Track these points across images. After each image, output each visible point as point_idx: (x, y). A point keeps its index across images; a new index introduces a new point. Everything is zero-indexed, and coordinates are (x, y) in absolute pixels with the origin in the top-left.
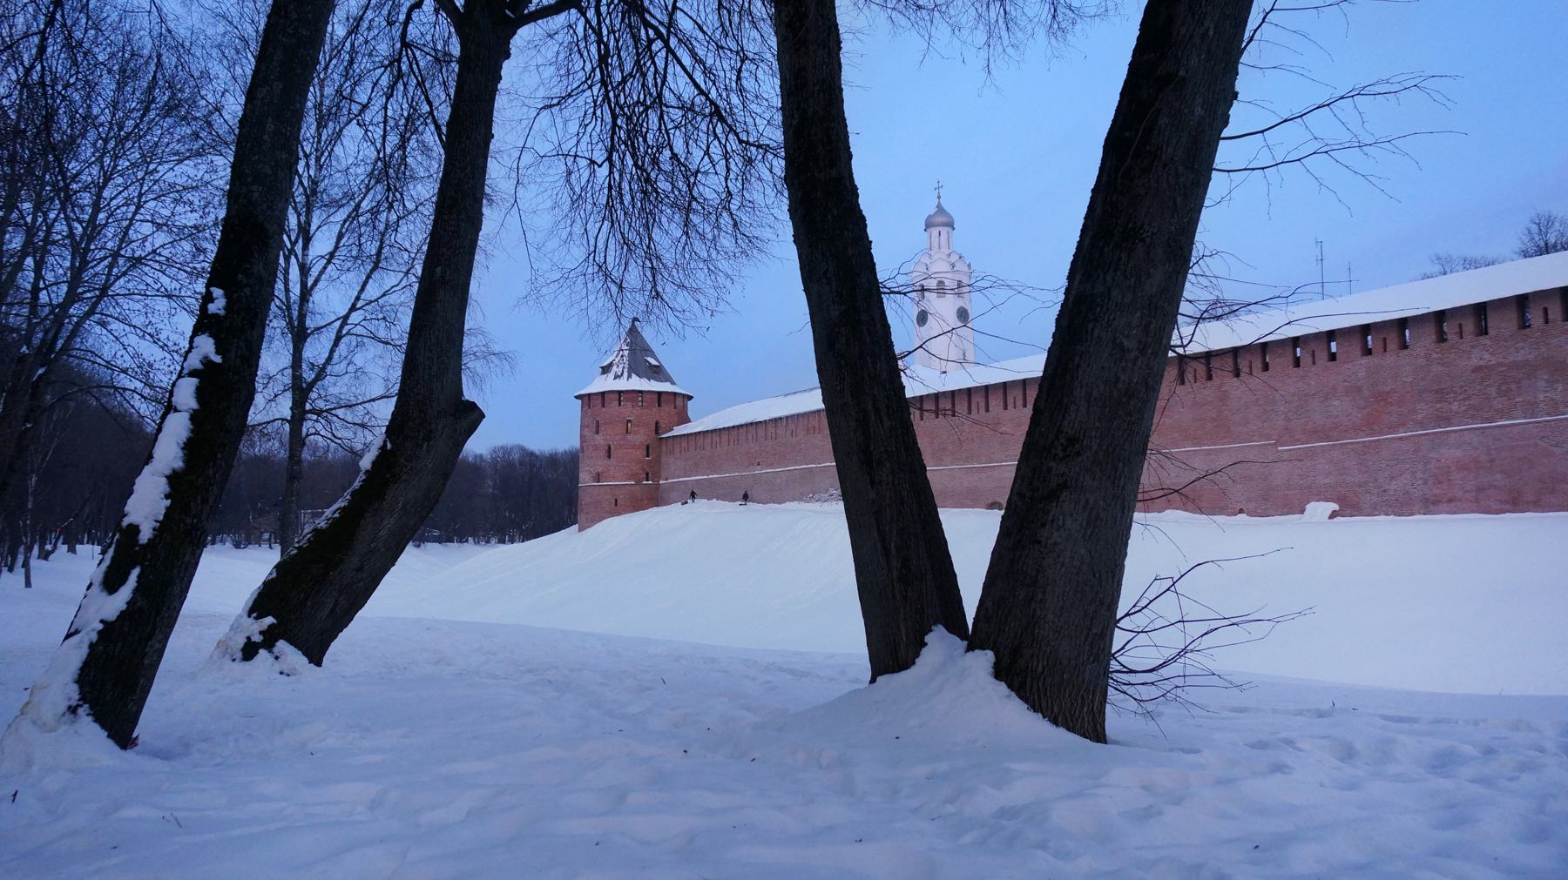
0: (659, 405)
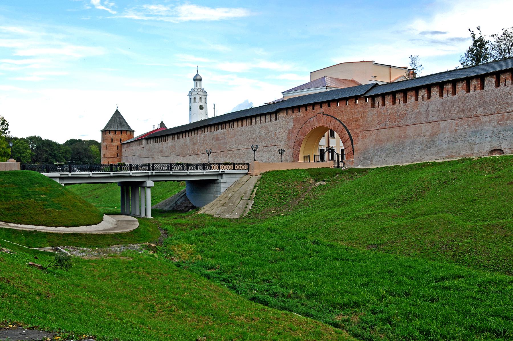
0: (121, 134)
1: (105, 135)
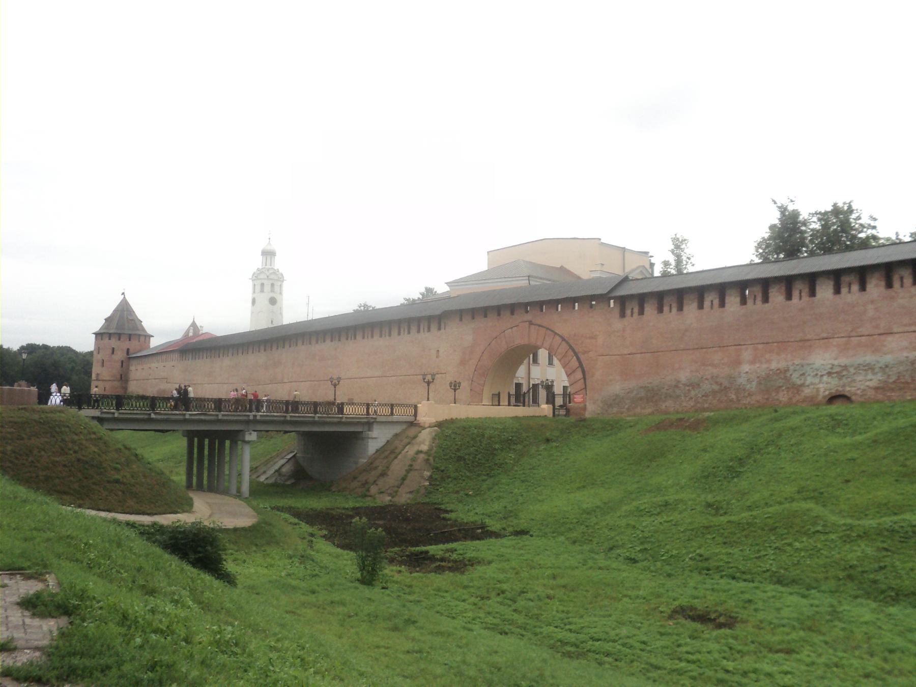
0: (130, 340)
1: (102, 342)
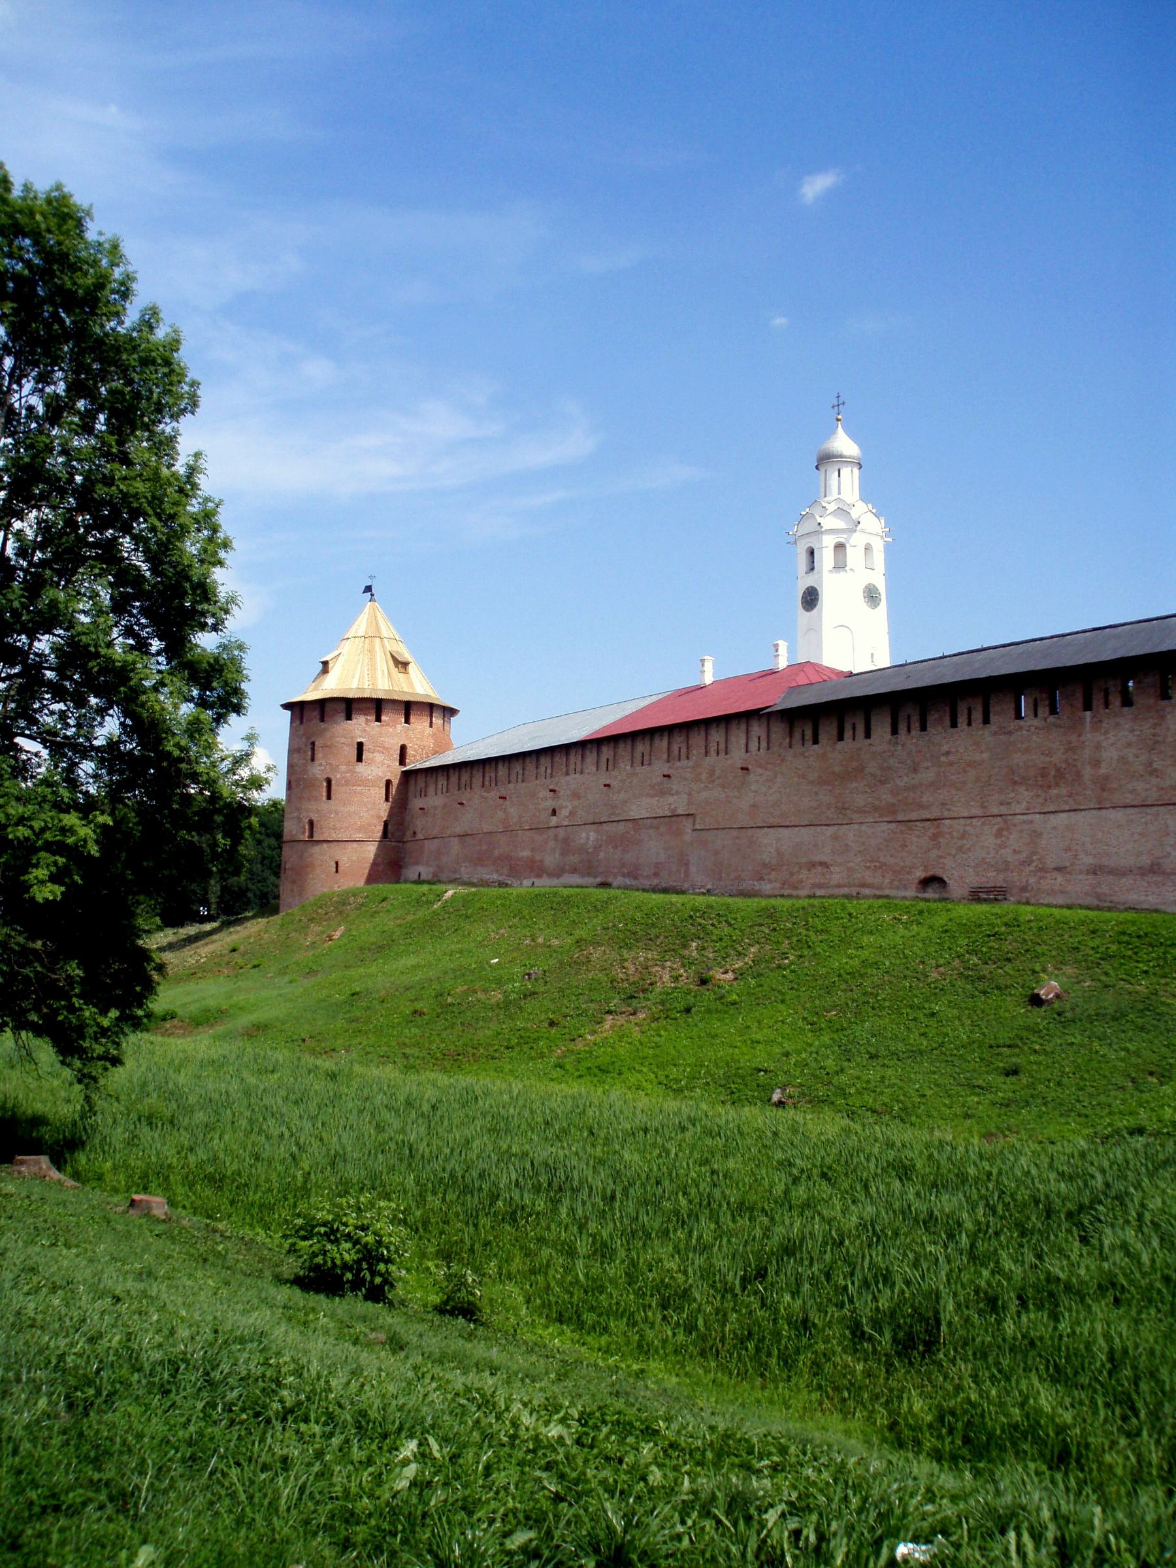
0: (407, 721)
1: (323, 725)
